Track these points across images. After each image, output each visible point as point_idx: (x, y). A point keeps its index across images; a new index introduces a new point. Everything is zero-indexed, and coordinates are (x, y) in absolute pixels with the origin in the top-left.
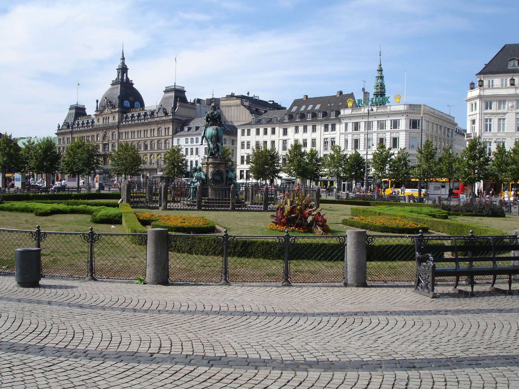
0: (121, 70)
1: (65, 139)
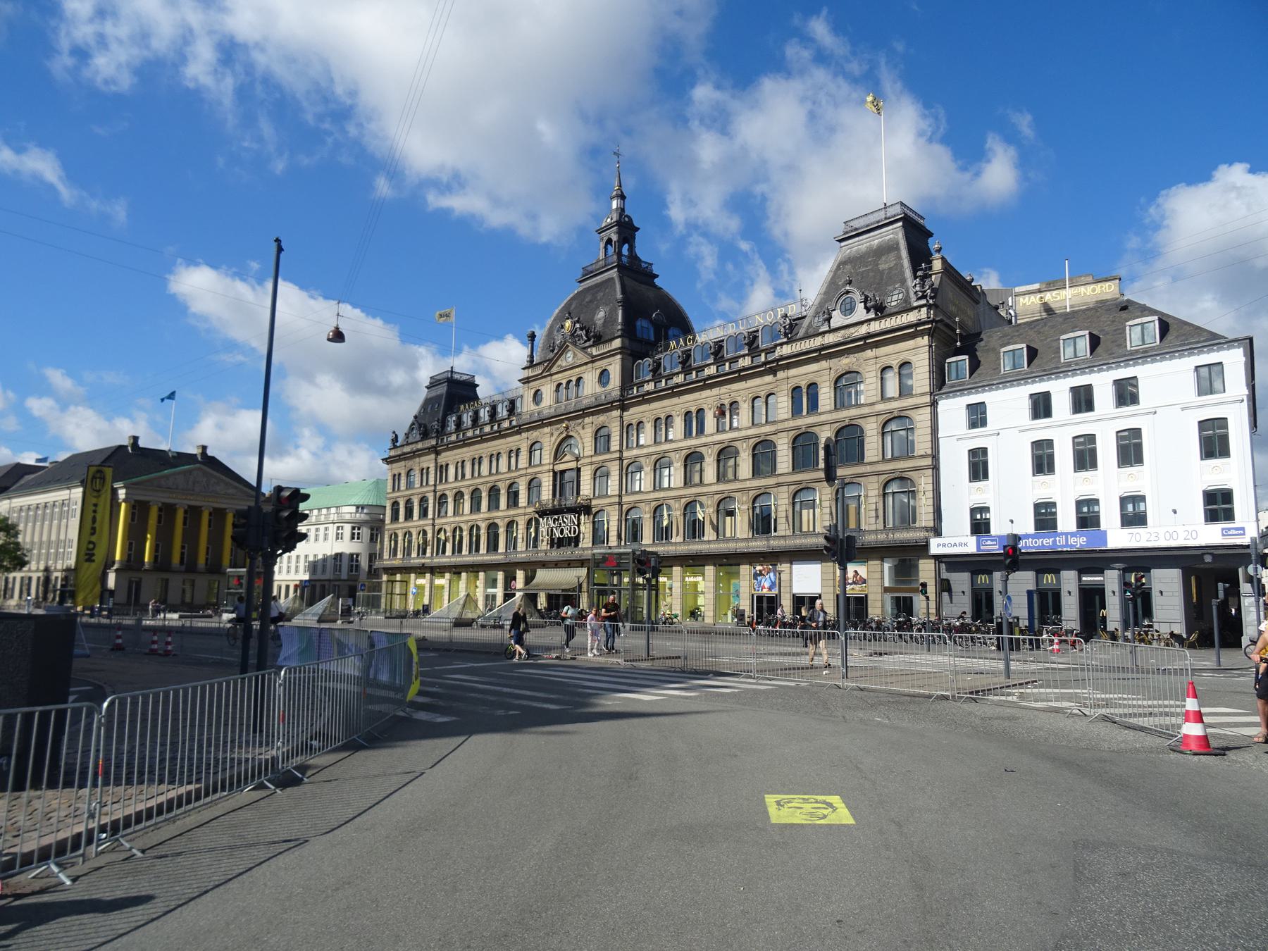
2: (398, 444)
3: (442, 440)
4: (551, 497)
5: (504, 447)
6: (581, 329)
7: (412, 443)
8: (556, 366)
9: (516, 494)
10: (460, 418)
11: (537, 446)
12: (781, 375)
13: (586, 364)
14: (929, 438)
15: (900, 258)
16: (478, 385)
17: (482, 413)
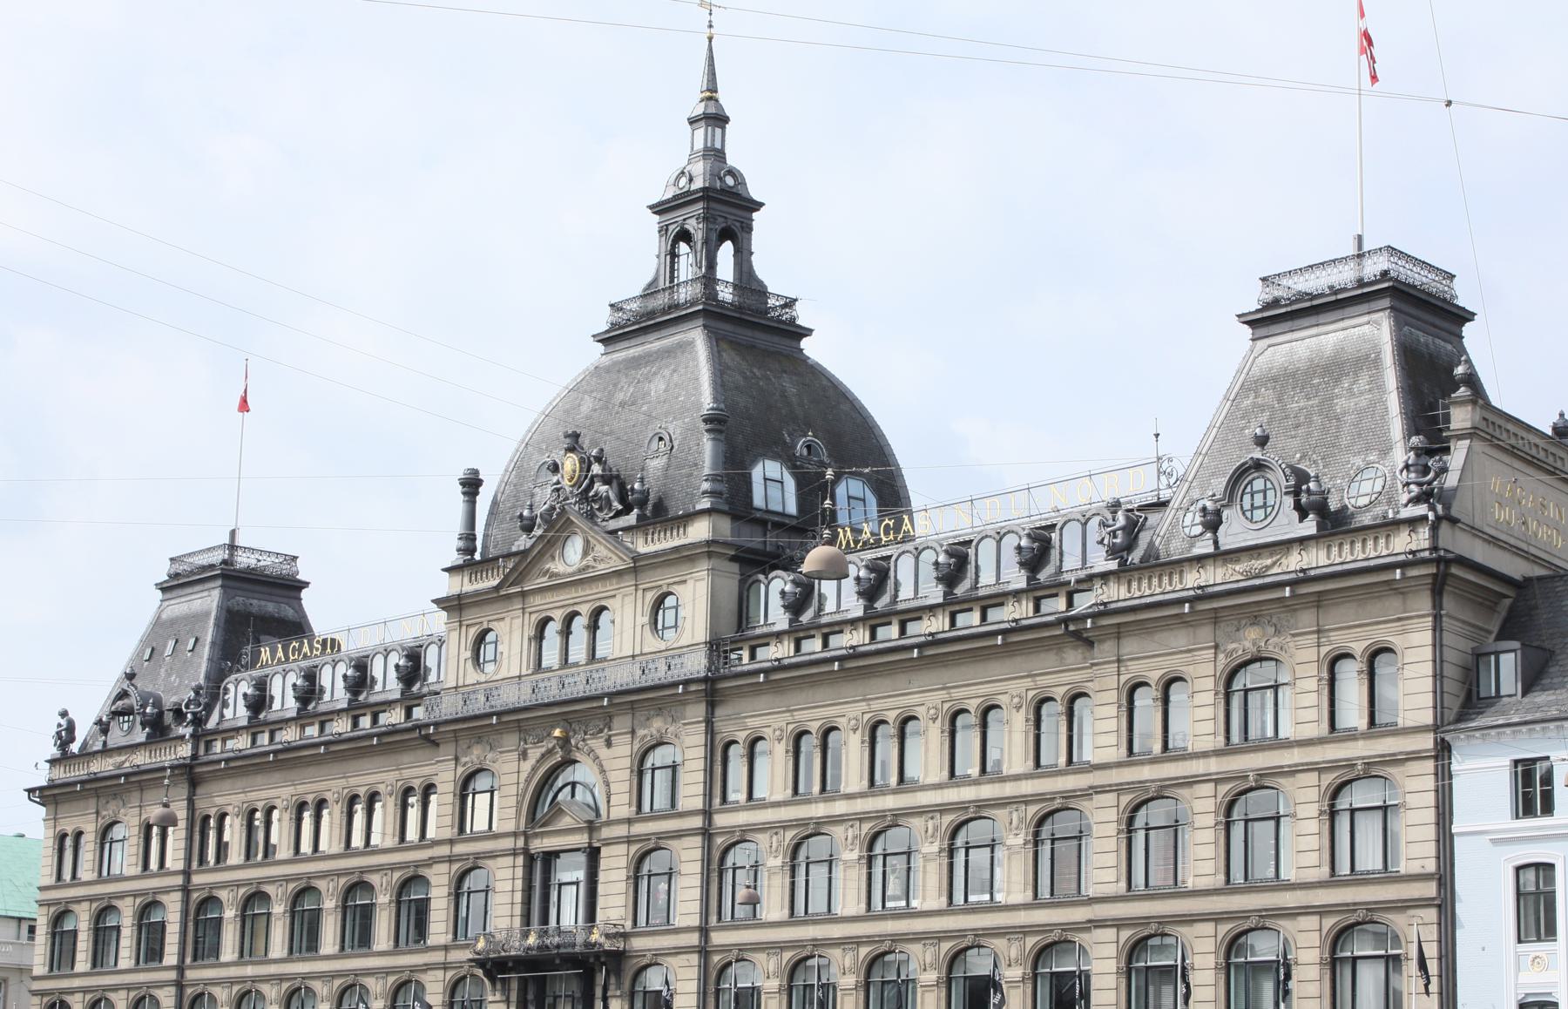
0: (698, 208)
1: (117, 832)
2: (75, 747)
3: (208, 745)
4: (517, 922)
5: (391, 777)
6: (607, 480)
7: (120, 750)
8: (536, 571)
9: (421, 911)
10: (261, 686)
11: (482, 782)
12: (1106, 650)
13: (618, 574)
14: (1430, 832)
15: (1379, 387)
16: (306, 584)
17: (325, 679)
